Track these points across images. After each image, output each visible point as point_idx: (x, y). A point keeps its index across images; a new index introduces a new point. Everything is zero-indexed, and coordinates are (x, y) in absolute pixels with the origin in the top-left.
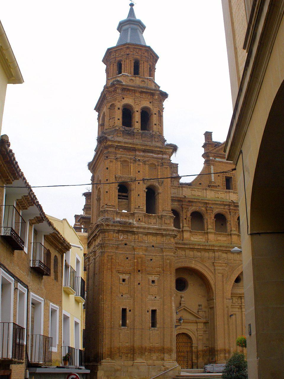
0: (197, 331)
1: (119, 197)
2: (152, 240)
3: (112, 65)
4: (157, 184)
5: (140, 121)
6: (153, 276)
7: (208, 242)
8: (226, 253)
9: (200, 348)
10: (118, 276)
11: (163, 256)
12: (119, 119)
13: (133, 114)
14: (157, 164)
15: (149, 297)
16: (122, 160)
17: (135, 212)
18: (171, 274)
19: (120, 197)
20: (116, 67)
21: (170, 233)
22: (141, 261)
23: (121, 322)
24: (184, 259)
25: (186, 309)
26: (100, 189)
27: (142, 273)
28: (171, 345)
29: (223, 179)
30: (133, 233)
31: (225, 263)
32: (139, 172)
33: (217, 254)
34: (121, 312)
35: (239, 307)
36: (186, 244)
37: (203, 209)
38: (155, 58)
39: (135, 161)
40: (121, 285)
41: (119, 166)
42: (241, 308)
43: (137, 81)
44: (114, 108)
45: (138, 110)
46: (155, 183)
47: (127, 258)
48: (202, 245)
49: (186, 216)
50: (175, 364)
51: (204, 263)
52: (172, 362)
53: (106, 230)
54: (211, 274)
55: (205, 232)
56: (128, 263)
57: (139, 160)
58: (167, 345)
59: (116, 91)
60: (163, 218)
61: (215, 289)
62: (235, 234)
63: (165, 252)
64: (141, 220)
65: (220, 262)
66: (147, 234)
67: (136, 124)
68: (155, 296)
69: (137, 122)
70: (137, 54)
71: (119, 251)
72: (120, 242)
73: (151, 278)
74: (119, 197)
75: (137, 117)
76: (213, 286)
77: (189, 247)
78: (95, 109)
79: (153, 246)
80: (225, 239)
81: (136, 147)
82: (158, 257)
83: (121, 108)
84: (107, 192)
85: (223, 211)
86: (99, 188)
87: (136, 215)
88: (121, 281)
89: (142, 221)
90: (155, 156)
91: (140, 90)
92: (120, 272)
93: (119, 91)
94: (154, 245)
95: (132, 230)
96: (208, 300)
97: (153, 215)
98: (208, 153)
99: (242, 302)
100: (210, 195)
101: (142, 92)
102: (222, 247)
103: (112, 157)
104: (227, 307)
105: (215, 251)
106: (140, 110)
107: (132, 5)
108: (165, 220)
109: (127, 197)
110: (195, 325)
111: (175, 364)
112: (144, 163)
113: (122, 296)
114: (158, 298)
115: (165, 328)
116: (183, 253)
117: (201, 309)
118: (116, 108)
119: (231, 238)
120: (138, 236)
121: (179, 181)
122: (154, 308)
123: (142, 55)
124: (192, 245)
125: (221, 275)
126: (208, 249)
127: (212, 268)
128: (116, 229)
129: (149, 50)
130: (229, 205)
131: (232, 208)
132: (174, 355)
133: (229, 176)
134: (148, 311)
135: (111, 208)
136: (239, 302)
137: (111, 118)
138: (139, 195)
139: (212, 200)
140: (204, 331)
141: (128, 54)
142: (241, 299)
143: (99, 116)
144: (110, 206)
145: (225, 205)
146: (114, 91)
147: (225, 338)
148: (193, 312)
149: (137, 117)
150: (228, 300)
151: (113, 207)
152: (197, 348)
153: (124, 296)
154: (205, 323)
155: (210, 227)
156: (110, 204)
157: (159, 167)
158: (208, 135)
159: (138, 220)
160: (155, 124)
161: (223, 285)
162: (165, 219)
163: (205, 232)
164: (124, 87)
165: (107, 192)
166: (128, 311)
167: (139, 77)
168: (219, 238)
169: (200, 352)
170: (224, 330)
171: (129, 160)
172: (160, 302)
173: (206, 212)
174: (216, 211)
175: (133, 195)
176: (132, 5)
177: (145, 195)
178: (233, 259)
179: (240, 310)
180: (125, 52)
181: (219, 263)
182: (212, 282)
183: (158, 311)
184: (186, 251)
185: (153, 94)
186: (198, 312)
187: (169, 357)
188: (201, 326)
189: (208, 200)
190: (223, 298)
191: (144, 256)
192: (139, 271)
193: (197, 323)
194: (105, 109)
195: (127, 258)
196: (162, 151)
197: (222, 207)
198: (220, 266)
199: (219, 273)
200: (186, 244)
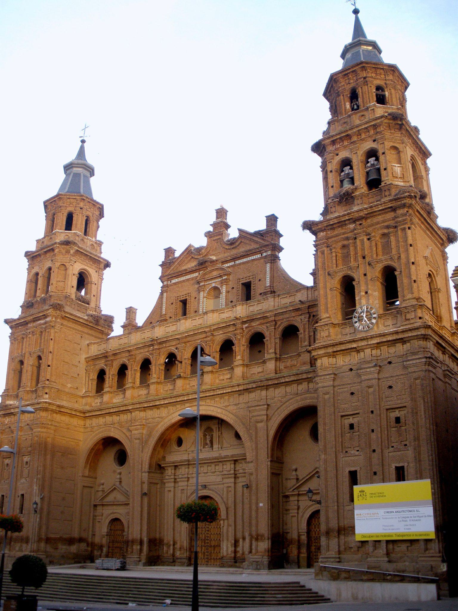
24: (104, 427)
30: (12, 414)
36: (102, 410)
57: (30, 333)
65: (137, 424)
72: (6, 427)
73: (26, 459)
79: (28, 424)
90: (42, 322)
91: (42, 251)
92: (4, 457)
102: (134, 404)
107: (83, 142)
142: (175, 469)
176: (83, 142)
183: (25, 495)
196: (44, 315)
197: (146, 350)
199: (136, 439)
200: (102, 410)
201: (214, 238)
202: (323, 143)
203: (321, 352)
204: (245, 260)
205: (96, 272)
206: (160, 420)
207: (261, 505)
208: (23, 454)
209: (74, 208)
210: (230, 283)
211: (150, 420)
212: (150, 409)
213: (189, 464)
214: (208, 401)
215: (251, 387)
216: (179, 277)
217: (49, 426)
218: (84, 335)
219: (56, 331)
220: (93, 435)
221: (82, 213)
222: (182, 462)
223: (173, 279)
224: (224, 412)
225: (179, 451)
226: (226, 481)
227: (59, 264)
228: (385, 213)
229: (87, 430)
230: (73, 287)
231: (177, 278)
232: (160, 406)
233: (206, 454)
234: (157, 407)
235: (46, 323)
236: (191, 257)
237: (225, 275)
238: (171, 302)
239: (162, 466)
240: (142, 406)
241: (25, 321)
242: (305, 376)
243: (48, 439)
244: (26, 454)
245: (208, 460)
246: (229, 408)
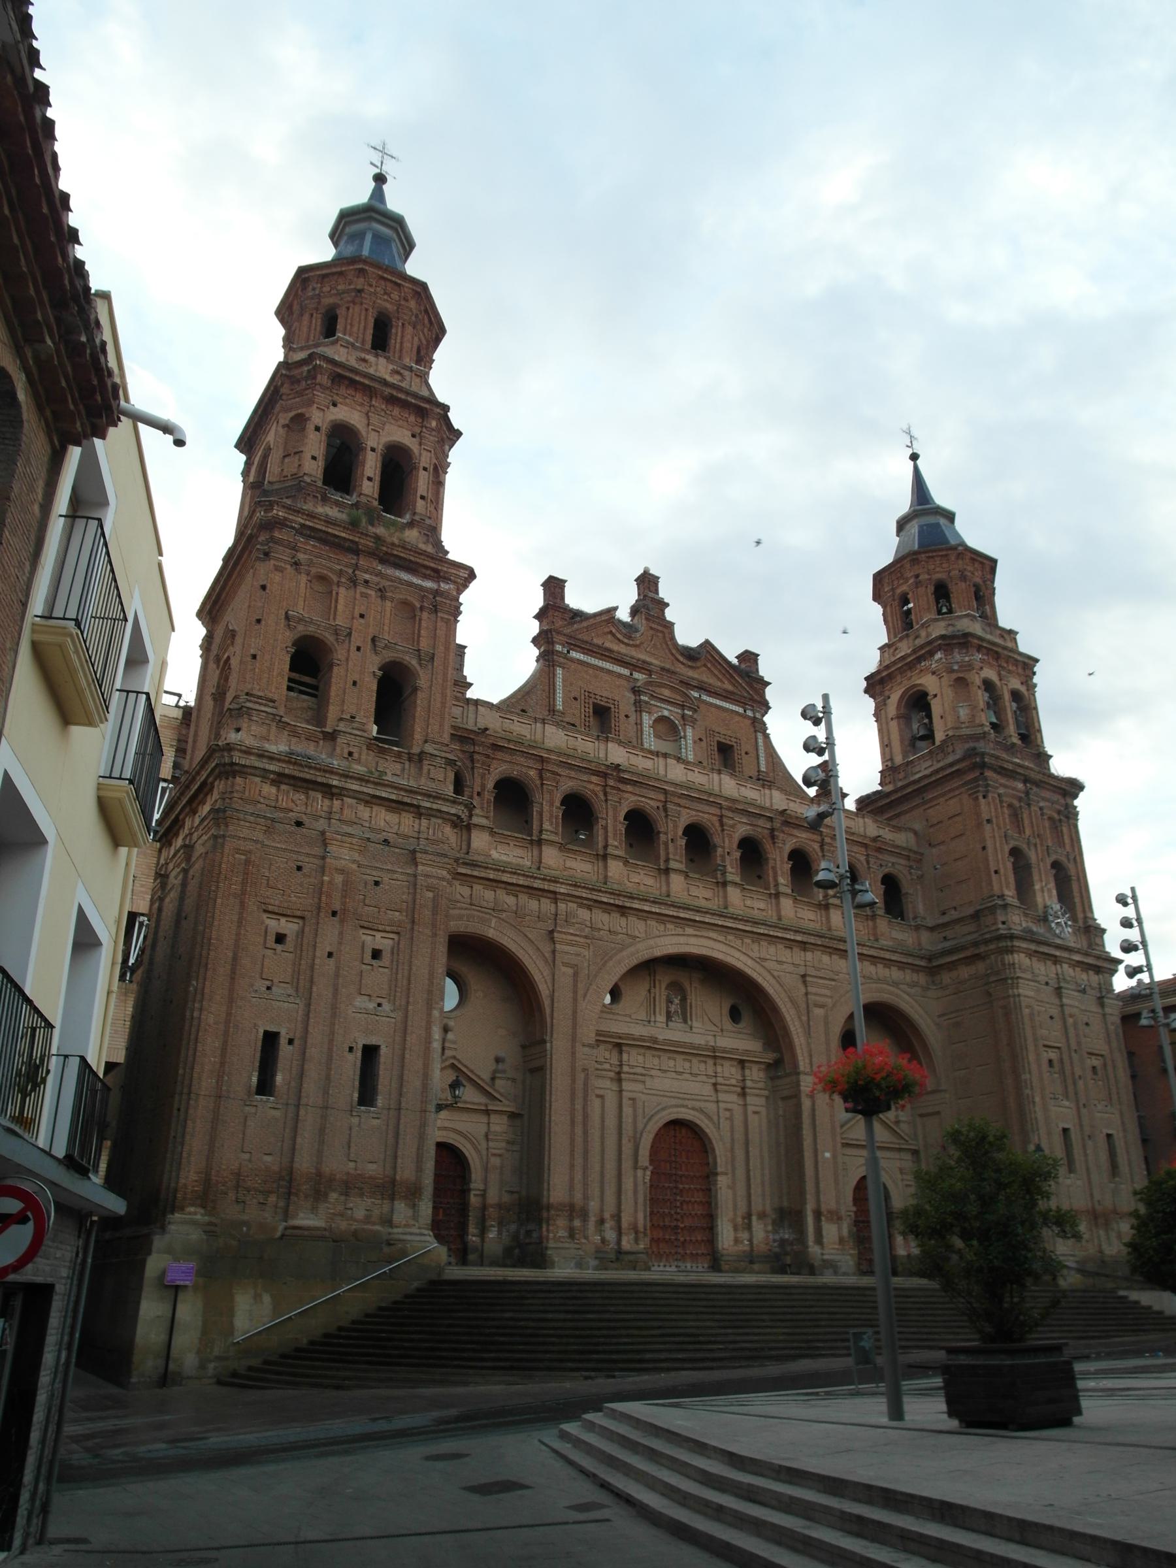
0: (487, 1140)
1: (291, 684)
2: (383, 818)
3: (306, 317)
4: (414, 662)
5: (377, 479)
6: (379, 935)
7: (539, 869)
8: (589, 908)
9: (493, 1197)
10: (263, 923)
11: (415, 876)
12: (314, 458)
13: (357, 455)
14: (418, 605)
15: (361, 1002)
16: (314, 570)
17: (338, 728)
18: (435, 935)
19: (293, 685)
20: (319, 324)
21: (444, 809)
22: (346, 883)
23: (255, 1079)
24: (466, 909)
25: (460, 1066)
26: (232, 658)
27: (342, 921)
28: (419, 1169)
29: (587, 710)
31: (586, 937)
32: (362, 616)
33: (562, 906)
34: (260, 1044)
35: (612, 1074)
37: (532, 773)
38: (436, 331)
39: (354, 582)
40: (269, 952)
41: (303, 585)
42: (620, 1080)
43: (381, 367)
44: (303, 429)
45: (375, 446)
46: (407, 658)
47: (299, 868)
48: (524, 875)
49: (483, 786)
50: (428, 1238)
51: (523, 929)
52: (418, 1231)
53: (237, 768)
54: (541, 964)
55: (532, 840)
56: (301, 885)
57: (366, 582)
58: (406, 1172)
59: (315, 378)
60: (425, 762)
61: (552, 1011)
62: (617, 857)
63: (424, 864)
64: (356, 755)
65: (571, 931)
66: (372, 801)
67: (366, 483)
68: (379, 1000)
69: (370, 479)
70: (386, 297)
71: (274, 840)
74: (291, 684)
75: (371, 466)
76: (547, 1003)
77: (483, 875)
78: (237, 446)
79: (386, 842)
80: (587, 867)
81: (362, 541)
82: (400, 877)
83: (324, 427)
84: (254, 657)
86: (228, 658)
87: (341, 740)
88: (271, 938)
89: (359, 761)
92: (270, 908)
93: (323, 379)
94: (391, 840)
95: (324, 780)
96: (523, 1047)
97: (395, 749)
98: (550, 631)
99: (621, 1061)
100: (555, 738)
101: (392, 400)
102: (579, 887)
103: (282, 554)
104: (584, 1070)
105: (558, 896)
106: (380, 447)
107: (380, 179)
108: (429, 770)
109: (316, 688)
110: (484, 1119)
111: (428, 1238)
112: (382, 592)
113: (268, 988)
114: (387, 1006)
115: (403, 1112)
116: (466, 891)
117: (504, 1071)
118: (310, 427)
119: (606, 867)
120: (343, 805)
121: (464, 694)
122: (373, 1040)
123: (403, 302)
124: (495, 870)
125: (570, 971)
126: (540, 890)
127: (546, 949)
128: (272, 768)
129: (421, 290)
130: (605, 775)
131: (611, 782)
132: (426, 1208)
133: (602, 703)
134: (351, 1049)
135: (260, 704)
136: (615, 1061)
137: (293, 452)
138: (355, 683)
139: (560, 754)
140: (508, 1142)
141: (360, 291)
143: (248, 464)
144: (260, 697)
146: (306, 379)
147: (572, 1166)
148: (479, 1077)
149: (371, 466)
150: (586, 1049)
151: (271, 704)
152: (483, 1195)
153: (274, 989)
154: (513, 1116)
155: (546, 826)
156: (260, 694)
157: (425, 615)
158: (554, 587)
159: (346, 756)
160: (422, 497)
161: (575, 1000)
162: (432, 768)
163: (534, 838)
164: (339, 370)
165: (254, 657)
166: (283, 1041)
167: (388, 358)
168: (569, 863)
169: (491, 1210)
170: (572, 1141)
171: (335, 578)
172: (393, 1020)
173: (538, 782)
174: (568, 785)
175: (338, 679)
177: (375, 687)
178: (606, 928)
179: (615, 1087)
180: (350, 284)
181: (564, 933)
182: (544, 989)
183: (383, 1050)
184: (476, 887)
185: (422, 413)
186: (493, 1079)
187: (410, 1212)
188: (499, 1125)
189: (549, 751)
190: (574, 1039)
191: (354, 866)
192: (334, 914)
193: (487, 1112)
194: (273, 435)
195: (299, 868)
196: (436, 571)
198: (568, 944)
199: (565, 964)
201: (653, 626)
202: (970, 639)
203: (1024, 945)
204: (718, 702)
206: (629, 941)
207: (827, 1155)
208: (362, 923)
211: (602, 932)
212: (605, 911)
213: (649, 1048)
214: (730, 937)
215: (813, 941)
216: (587, 654)
222: (644, 1041)
223: (576, 651)
224: (758, 968)
225: (614, 1014)
226: (722, 1096)
228: (1054, 792)
231: (583, 653)
232: (631, 912)
233: (676, 1033)
234: (627, 911)
235: (437, 593)
236: (606, 630)
237: (690, 709)
241: (356, 543)
242: (887, 955)
244: (381, 928)
245: (694, 1048)
246: (765, 964)
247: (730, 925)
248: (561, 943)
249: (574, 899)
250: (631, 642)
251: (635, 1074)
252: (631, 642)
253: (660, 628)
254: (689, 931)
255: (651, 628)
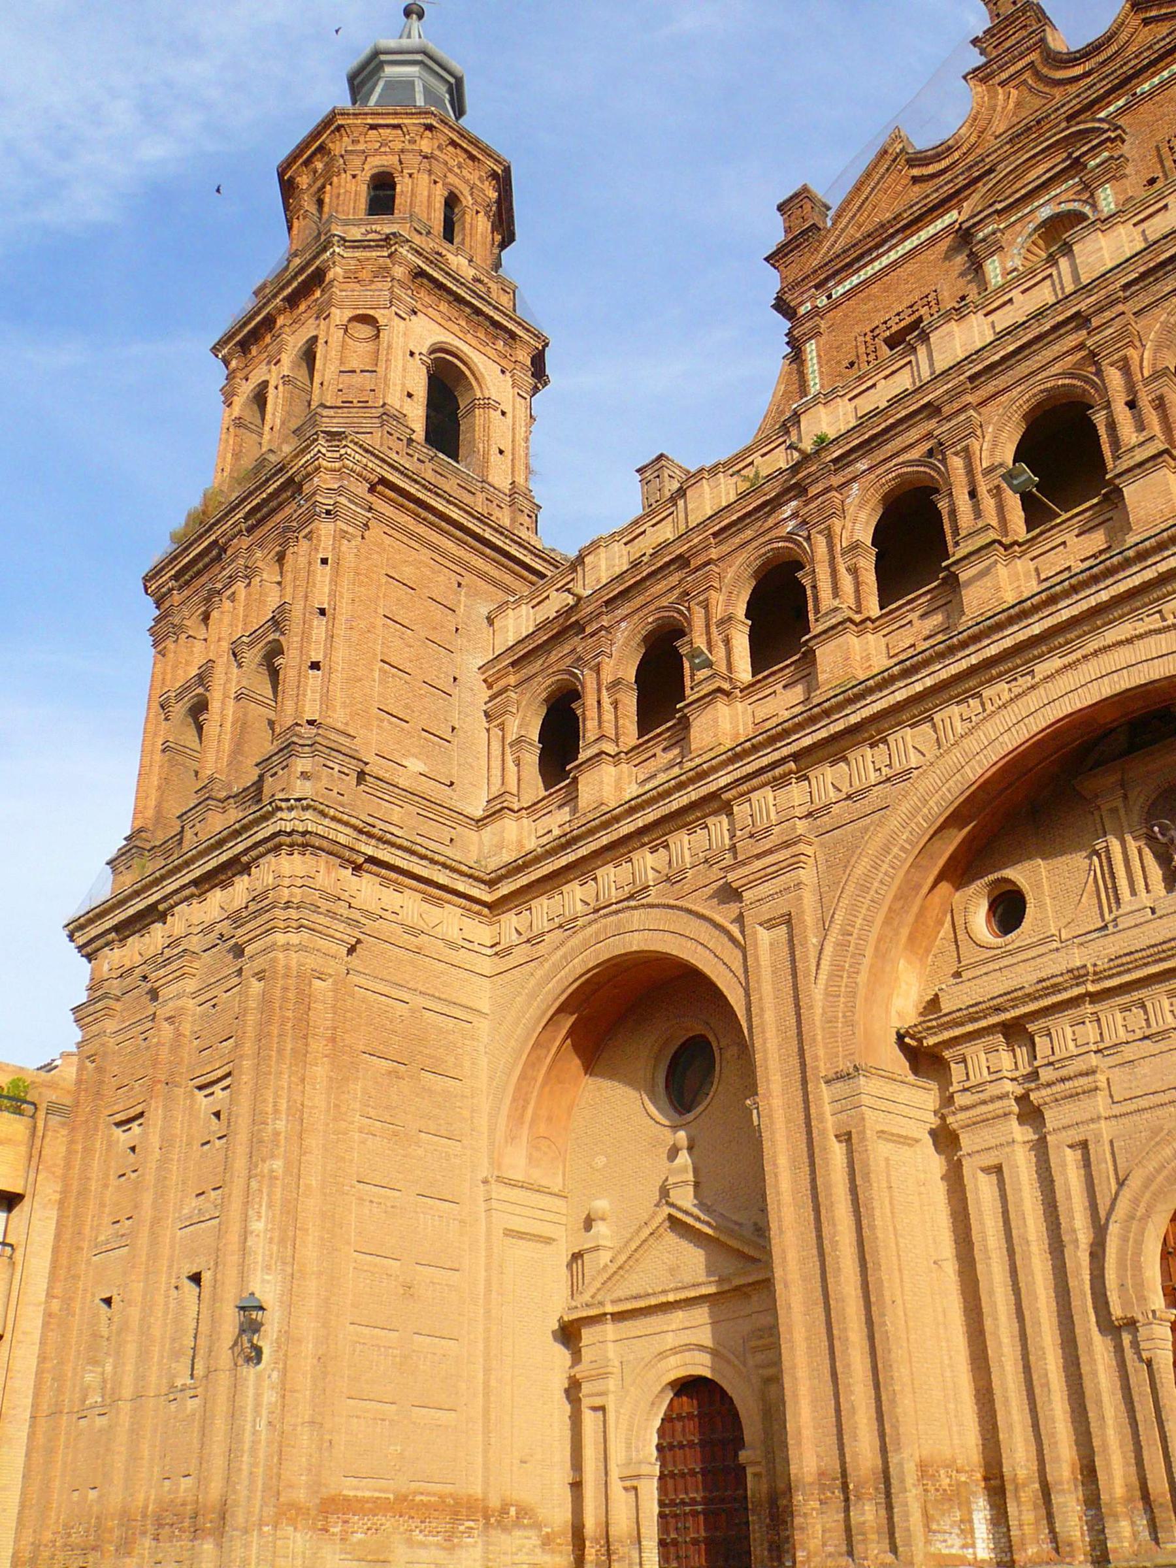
85: (770, 541)
133: (902, 324)
145: (774, 504)
182: (735, 998)
201: (1004, 76)
205: (503, 372)
209: (395, 159)
210: (1129, 170)
211: (835, 809)
217: (322, 919)
218: (470, 577)
219: (345, 527)
220: (540, 973)
221: (430, 172)
222: (1056, 989)
227: (349, 314)
229: (511, 961)
230: (410, 395)
238: (846, 363)
239: (930, 1041)
240: (785, 751)
243: (317, 983)
247: (1137, 581)
248: (751, 884)
249: (755, 782)
250: (956, 155)
251: (1063, 1080)
252: (956, 155)
253: (1020, 65)
254: (1043, 668)
255: (1002, 84)
